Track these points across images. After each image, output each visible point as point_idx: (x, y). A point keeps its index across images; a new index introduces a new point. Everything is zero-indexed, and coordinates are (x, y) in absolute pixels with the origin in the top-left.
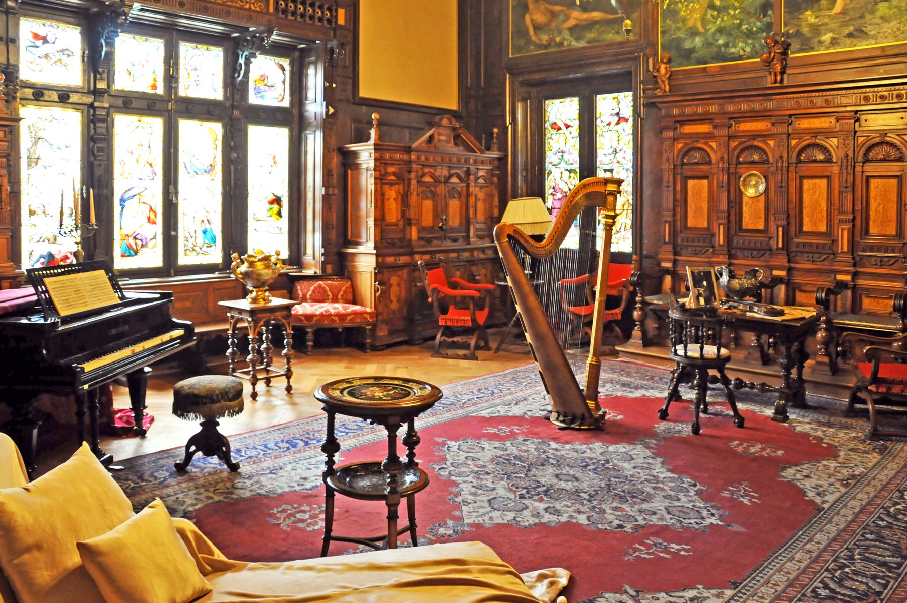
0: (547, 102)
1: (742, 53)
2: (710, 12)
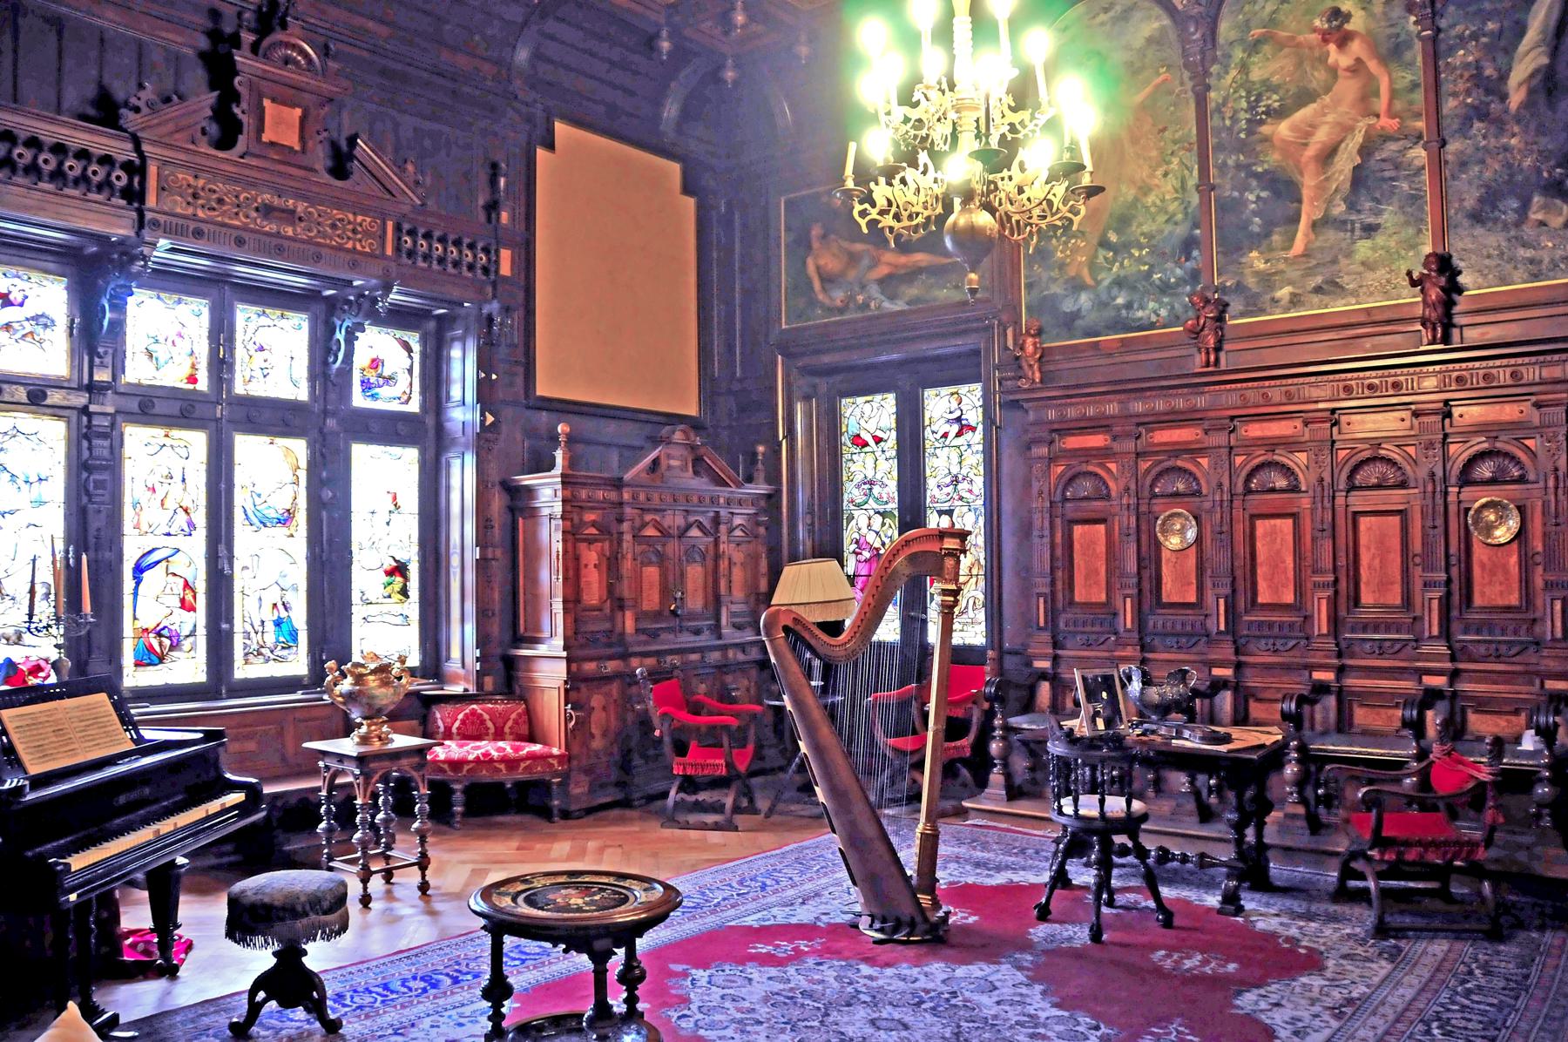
0: (843, 401)
1: (1154, 318)
2: (1102, 253)
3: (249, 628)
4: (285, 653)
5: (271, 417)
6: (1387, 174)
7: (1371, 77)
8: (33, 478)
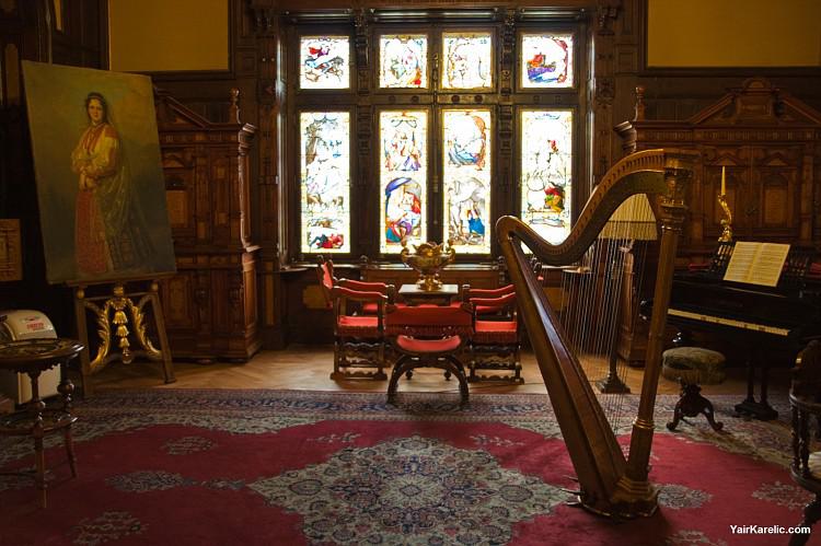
3: (453, 224)
4: (476, 240)
5: (402, 100)
8: (334, 143)
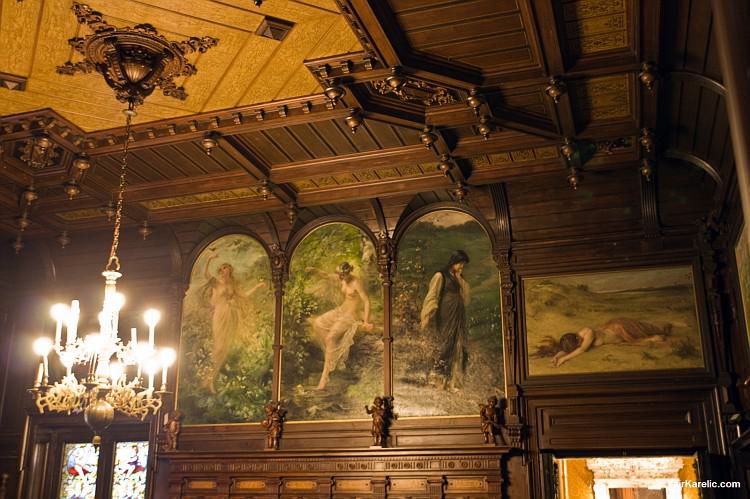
0: (67, 445)
2: (221, 376)
6: (366, 352)
7: (361, 301)
